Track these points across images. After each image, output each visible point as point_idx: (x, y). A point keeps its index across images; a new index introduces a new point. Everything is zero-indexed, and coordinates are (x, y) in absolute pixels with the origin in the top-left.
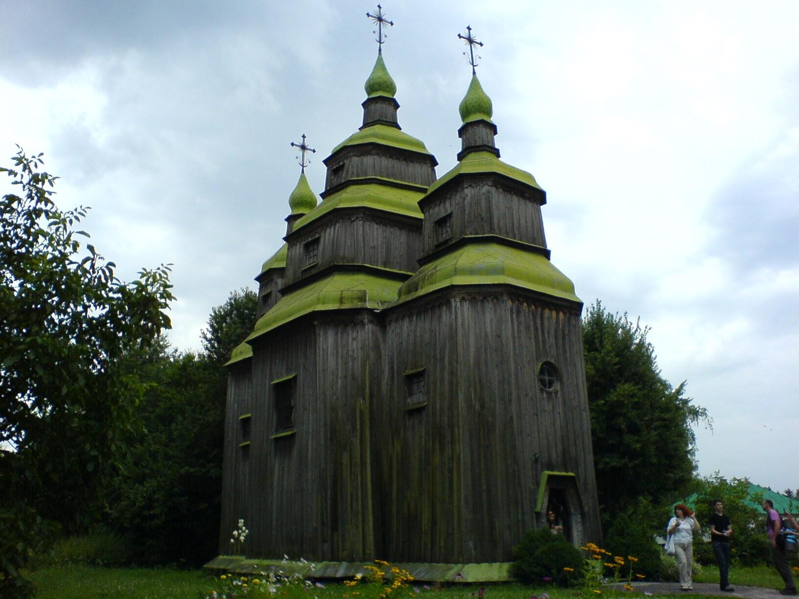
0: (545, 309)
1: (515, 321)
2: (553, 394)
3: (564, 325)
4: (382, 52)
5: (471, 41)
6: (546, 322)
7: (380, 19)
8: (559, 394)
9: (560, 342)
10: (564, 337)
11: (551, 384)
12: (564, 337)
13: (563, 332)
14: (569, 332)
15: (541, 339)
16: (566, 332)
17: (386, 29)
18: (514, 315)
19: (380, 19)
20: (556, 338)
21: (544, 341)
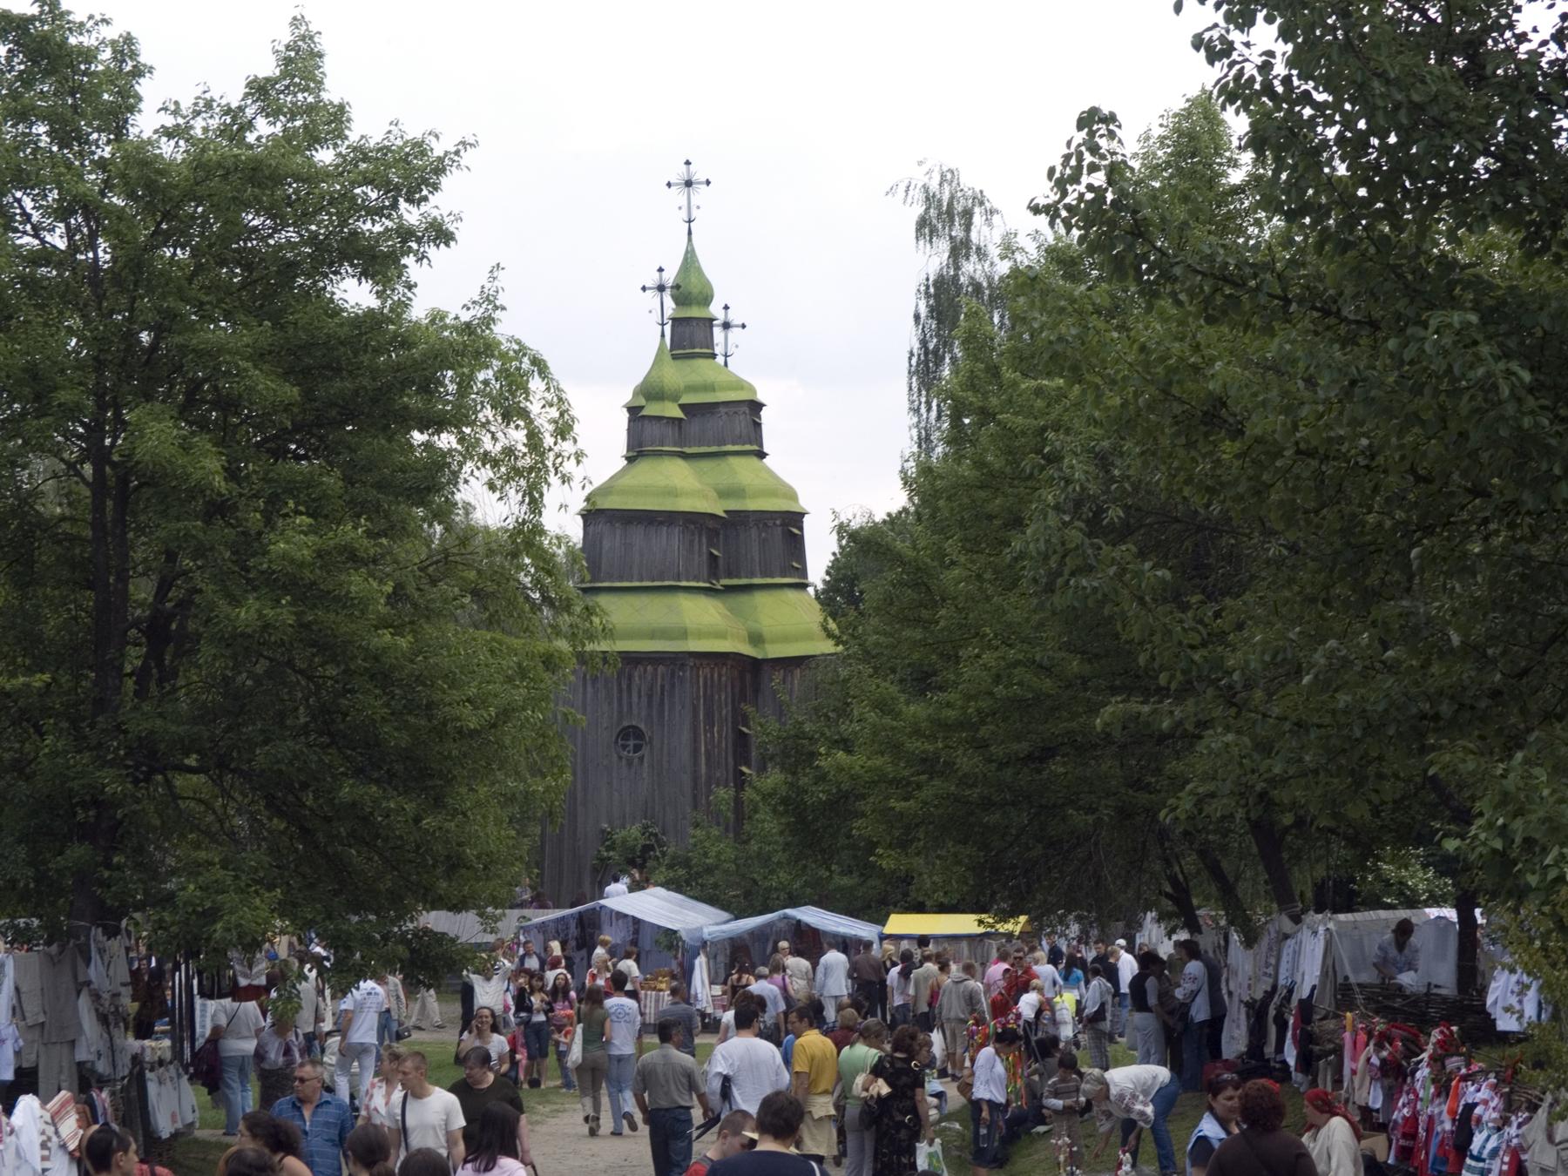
1: (589, 689)
2: (636, 761)
3: (663, 679)
4: (693, 236)
7: (689, 184)
8: (645, 760)
9: (656, 699)
10: (662, 694)
11: (637, 748)
12: (662, 694)
13: (663, 687)
15: (625, 702)
16: (667, 687)
17: (700, 194)
19: (689, 184)
20: (650, 697)
21: (630, 705)
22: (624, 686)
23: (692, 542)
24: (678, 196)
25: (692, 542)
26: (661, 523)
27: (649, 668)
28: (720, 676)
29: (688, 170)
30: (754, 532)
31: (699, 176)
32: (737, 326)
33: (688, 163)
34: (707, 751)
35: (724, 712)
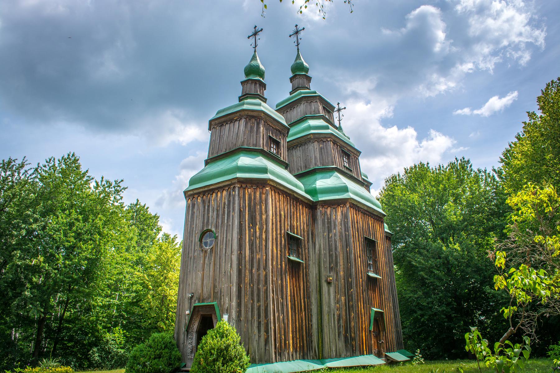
0: (212, 194)
3: (225, 199)
5: (255, 34)
6: (212, 202)
7: (297, 32)
10: (224, 207)
13: (225, 203)
14: (229, 201)
18: (191, 208)
20: (218, 211)
22: (206, 207)
23: (252, 128)
24: (294, 38)
25: (252, 128)
26: (236, 120)
27: (219, 194)
28: (261, 194)
29: (297, 28)
30: (316, 143)
31: (300, 27)
32: (343, 109)
33: (296, 26)
34: (250, 240)
35: (264, 217)
